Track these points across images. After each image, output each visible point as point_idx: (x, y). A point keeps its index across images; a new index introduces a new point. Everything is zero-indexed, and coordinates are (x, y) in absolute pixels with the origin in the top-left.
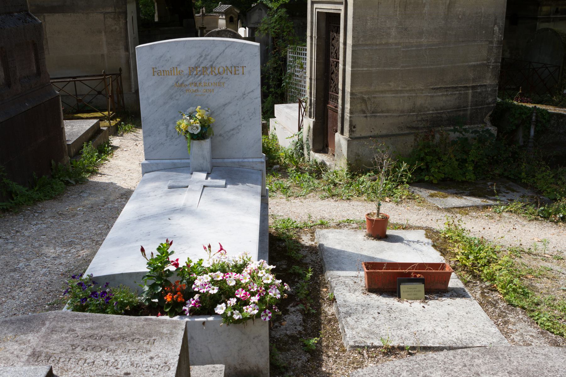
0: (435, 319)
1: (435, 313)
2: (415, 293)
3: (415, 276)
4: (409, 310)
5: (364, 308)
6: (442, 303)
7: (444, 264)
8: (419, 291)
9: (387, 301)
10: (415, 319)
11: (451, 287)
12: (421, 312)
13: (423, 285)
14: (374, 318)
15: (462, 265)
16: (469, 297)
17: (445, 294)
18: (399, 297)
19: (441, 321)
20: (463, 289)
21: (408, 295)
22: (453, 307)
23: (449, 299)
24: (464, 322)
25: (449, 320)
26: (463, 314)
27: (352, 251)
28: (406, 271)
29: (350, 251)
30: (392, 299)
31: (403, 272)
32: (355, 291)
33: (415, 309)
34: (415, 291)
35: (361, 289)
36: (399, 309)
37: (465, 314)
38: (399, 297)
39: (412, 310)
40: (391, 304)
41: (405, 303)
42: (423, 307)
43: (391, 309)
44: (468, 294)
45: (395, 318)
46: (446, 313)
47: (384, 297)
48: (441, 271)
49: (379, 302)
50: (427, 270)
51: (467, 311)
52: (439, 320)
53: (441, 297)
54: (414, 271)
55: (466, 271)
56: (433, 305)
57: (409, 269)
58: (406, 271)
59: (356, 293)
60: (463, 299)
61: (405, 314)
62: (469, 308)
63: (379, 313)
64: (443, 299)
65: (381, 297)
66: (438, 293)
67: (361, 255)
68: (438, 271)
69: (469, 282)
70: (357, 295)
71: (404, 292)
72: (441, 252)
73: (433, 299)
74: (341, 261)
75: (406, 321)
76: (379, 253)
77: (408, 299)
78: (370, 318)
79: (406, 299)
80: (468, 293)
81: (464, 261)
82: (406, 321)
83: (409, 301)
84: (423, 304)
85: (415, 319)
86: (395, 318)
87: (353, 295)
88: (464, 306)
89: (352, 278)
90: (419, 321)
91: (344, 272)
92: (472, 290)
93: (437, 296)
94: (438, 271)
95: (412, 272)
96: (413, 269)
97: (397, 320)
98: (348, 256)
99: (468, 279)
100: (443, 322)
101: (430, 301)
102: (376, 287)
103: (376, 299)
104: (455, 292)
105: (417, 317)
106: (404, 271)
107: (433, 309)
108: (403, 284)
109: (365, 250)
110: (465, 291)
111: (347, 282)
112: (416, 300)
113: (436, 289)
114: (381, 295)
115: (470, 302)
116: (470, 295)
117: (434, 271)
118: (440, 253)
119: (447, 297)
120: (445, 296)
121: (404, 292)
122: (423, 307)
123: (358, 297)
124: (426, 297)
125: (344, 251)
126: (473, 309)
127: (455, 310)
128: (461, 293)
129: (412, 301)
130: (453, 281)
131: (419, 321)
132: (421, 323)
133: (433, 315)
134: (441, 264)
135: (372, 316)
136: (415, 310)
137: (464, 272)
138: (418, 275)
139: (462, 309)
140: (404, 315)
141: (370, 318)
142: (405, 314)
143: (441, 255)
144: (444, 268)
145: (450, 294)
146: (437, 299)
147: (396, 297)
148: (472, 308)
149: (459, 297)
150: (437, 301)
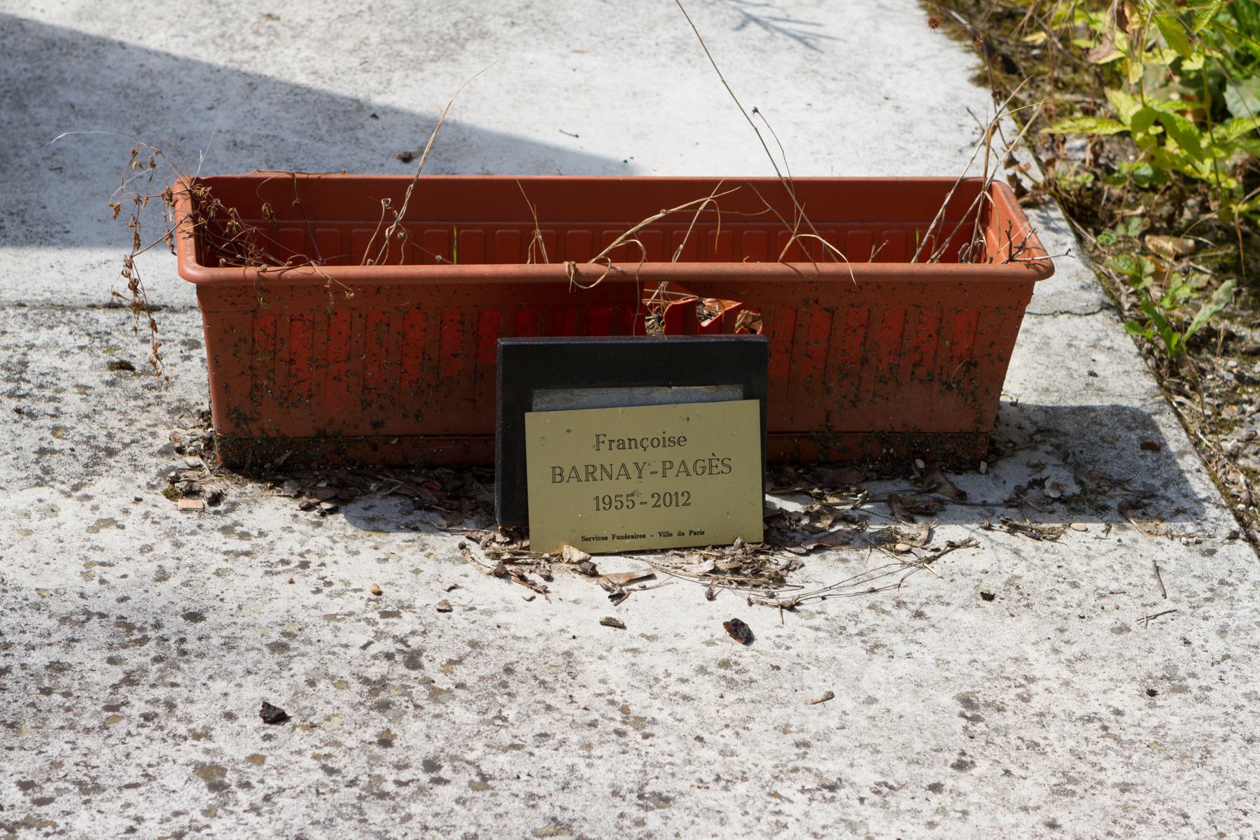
0: (832, 768)
1: (843, 701)
2: (674, 483)
3: (682, 319)
4: (591, 670)
5: (134, 658)
6: (920, 582)
7: (968, 188)
8: (711, 466)
9: (380, 575)
10: (628, 782)
11: (1030, 398)
12: (706, 689)
13: (754, 405)
14: (212, 776)
15: (1159, 174)
16: (1189, 509)
17: (964, 482)
18: (517, 526)
19: (884, 789)
20: (1142, 421)
21: (606, 503)
22: (1026, 619)
23: (1000, 534)
24: (1108, 798)
25: (964, 782)
26: (1116, 701)
27: (178, 48)
28: (590, 267)
29: (155, 41)
30: (445, 543)
31: (556, 285)
32: (92, 468)
33: (655, 660)
34: (667, 465)
35: (164, 436)
36: (491, 664)
37: (1129, 698)
38: (517, 526)
39: (616, 671)
40: (427, 599)
41: (568, 584)
42: (738, 630)
43: (413, 661)
44: (1179, 479)
45: (431, 765)
46: (947, 700)
47: (373, 523)
48: (933, 267)
49: (304, 585)
50: (796, 255)
51: (1153, 664)
52: (866, 776)
53: (929, 512)
54: (675, 266)
55: (1196, 229)
56: (832, 607)
57: (618, 256)
58: (590, 267)
59: (102, 485)
60: (1133, 532)
61: (542, 722)
62: (1177, 628)
63: (274, 716)
64: (946, 532)
65: (338, 521)
66: (896, 468)
67: (253, 84)
68: (913, 266)
69: (1203, 341)
70: (110, 509)
71: (558, 475)
72: (988, 50)
73: (844, 541)
74: (41, 140)
75: (532, 799)
76: (417, 65)
77: (596, 544)
78: (173, 777)
79: (583, 541)
80: (1190, 462)
81: (1171, 145)
82: (532, 799)
83: (611, 566)
84: (733, 603)
85: (627, 772)
86: (431, 765)
87: (69, 508)
88: (1130, 616)
89: (105, 319)
90: (663, 800)
91: (47, 256)
92: (1228, 426)
93: (891, 500)
94: (913, 266)
95: (652, 280)
96: (660, 246)
97: (446, 794)
98: (123, 91)
99: (1202, 317)
100: (902, 801)
101: (813, 563)
102: (300, 424)
103: (282, 550)
104: (1065, 457)
105: (663, 744)
106: (564, 267)
107: (826, 650)
108: (558, 396)
109: (298, 32)
110: (1154, 446)
111: (41, 361)
112: (681, 549)
113: (884, 438)
114: (340, 502)
115: (1197, 562)
116: (1201, 485)
117: (850, 268)
118: (974, 60)
119: (986, 513)
120: (961, 497)
121: (558, 475)
122: (738, 630)
123: (107, 536)
124: (773, 518)
125: (100, 45)
126: (1217, 646)
127: (1044, 666)
128: (1115, 470)
129: (641, 565)
130: (1058, 343)
131: (663, 800)
132: (678, 816)
133: (816, 721)
134: (944, 185)
135: (194, 752)
136: (644, 661)
137: (1168, 244)
138: (712, 308)
139: (1106, 643)
140: (527, 732)
141: (173, 777)
142: (542, 722)
143: (981, 80)
144: (966, 234)
145: (1014, 473)
146: (884, 541)
147: (489, 524)
148: (1204, 633)
149: (1100, 511)
150: (878, 559)
